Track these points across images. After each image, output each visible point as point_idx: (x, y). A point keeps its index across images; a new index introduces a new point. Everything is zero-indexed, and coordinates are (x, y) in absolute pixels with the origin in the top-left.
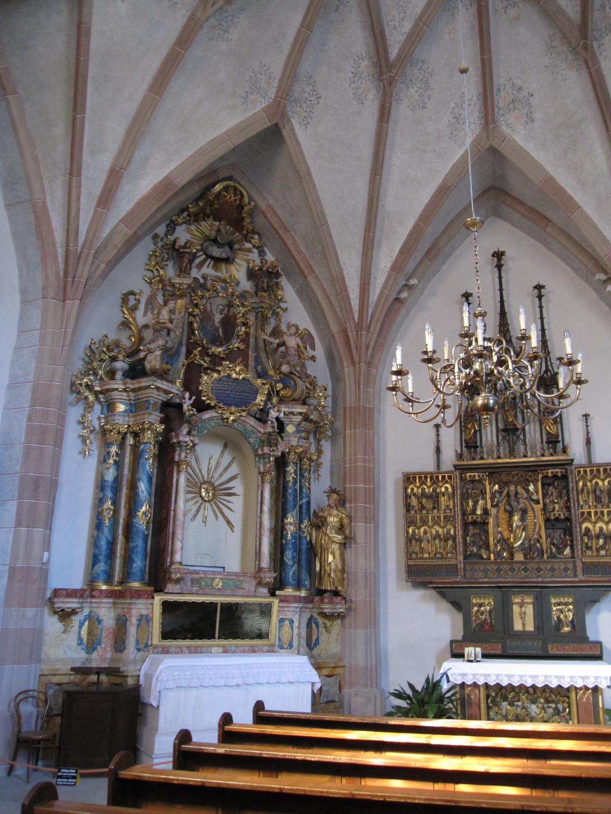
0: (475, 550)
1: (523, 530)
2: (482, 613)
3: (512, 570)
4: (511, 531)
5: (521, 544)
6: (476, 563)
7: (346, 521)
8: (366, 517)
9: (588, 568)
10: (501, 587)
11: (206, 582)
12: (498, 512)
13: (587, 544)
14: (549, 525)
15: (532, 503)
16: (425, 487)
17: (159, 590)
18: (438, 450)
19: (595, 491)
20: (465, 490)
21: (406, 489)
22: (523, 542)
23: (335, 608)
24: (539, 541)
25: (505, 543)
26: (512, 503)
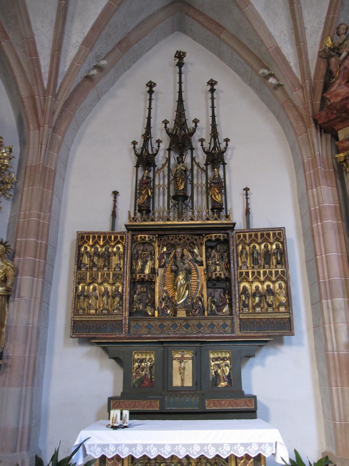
0: (141, 307)
1: (186, 289)
2: (143, 369)
3: (175, 326)
4: (175, 290)
5: (184, 301)
6: (141, 320)
7: (11, 273)
8: (34, 271)
9: (245, 324)
10: (162, 343)
12: (165, 272)
13: (244, 302)
14: (210, 285)
15: (197, 264)
16: (98, 246)
18: (114, 215)
19: (253, 253)
20: (135, 251)
21: (79, 247)
22: (186, 299)
24: (201, 300)
25: (170, 301)
26: (178, 264)
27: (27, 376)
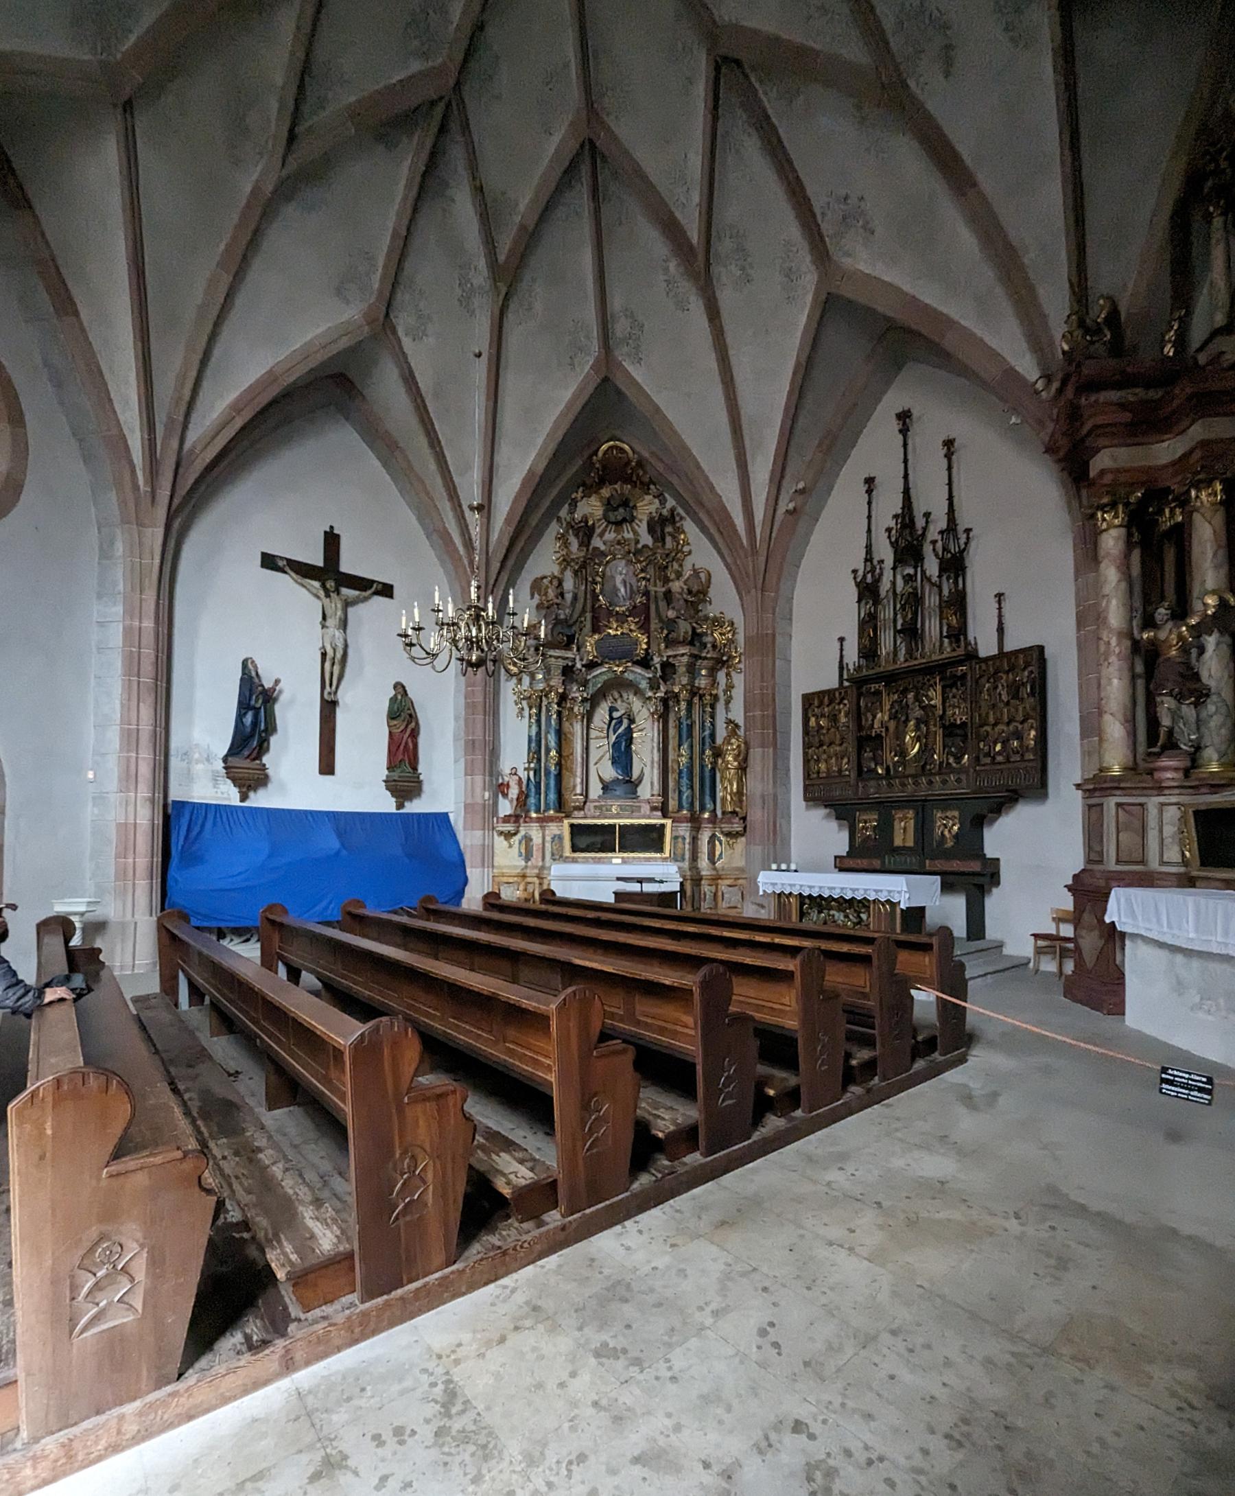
2: (867, 829)
17: (568, 816)
18: (841, 668)
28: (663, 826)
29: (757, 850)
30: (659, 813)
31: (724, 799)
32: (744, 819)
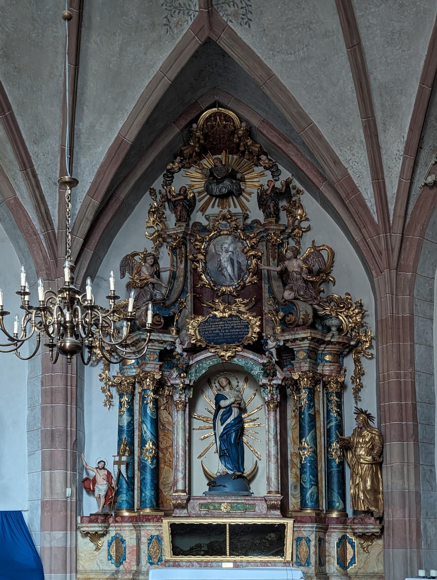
11: (214, 506)
17: (167, 515)
23: (367, 529)
27: (411, 539)
28: (283, 527)
29: (398, 553)
30: (278, 512)
31: (355, 497)
32: (381, 519)
